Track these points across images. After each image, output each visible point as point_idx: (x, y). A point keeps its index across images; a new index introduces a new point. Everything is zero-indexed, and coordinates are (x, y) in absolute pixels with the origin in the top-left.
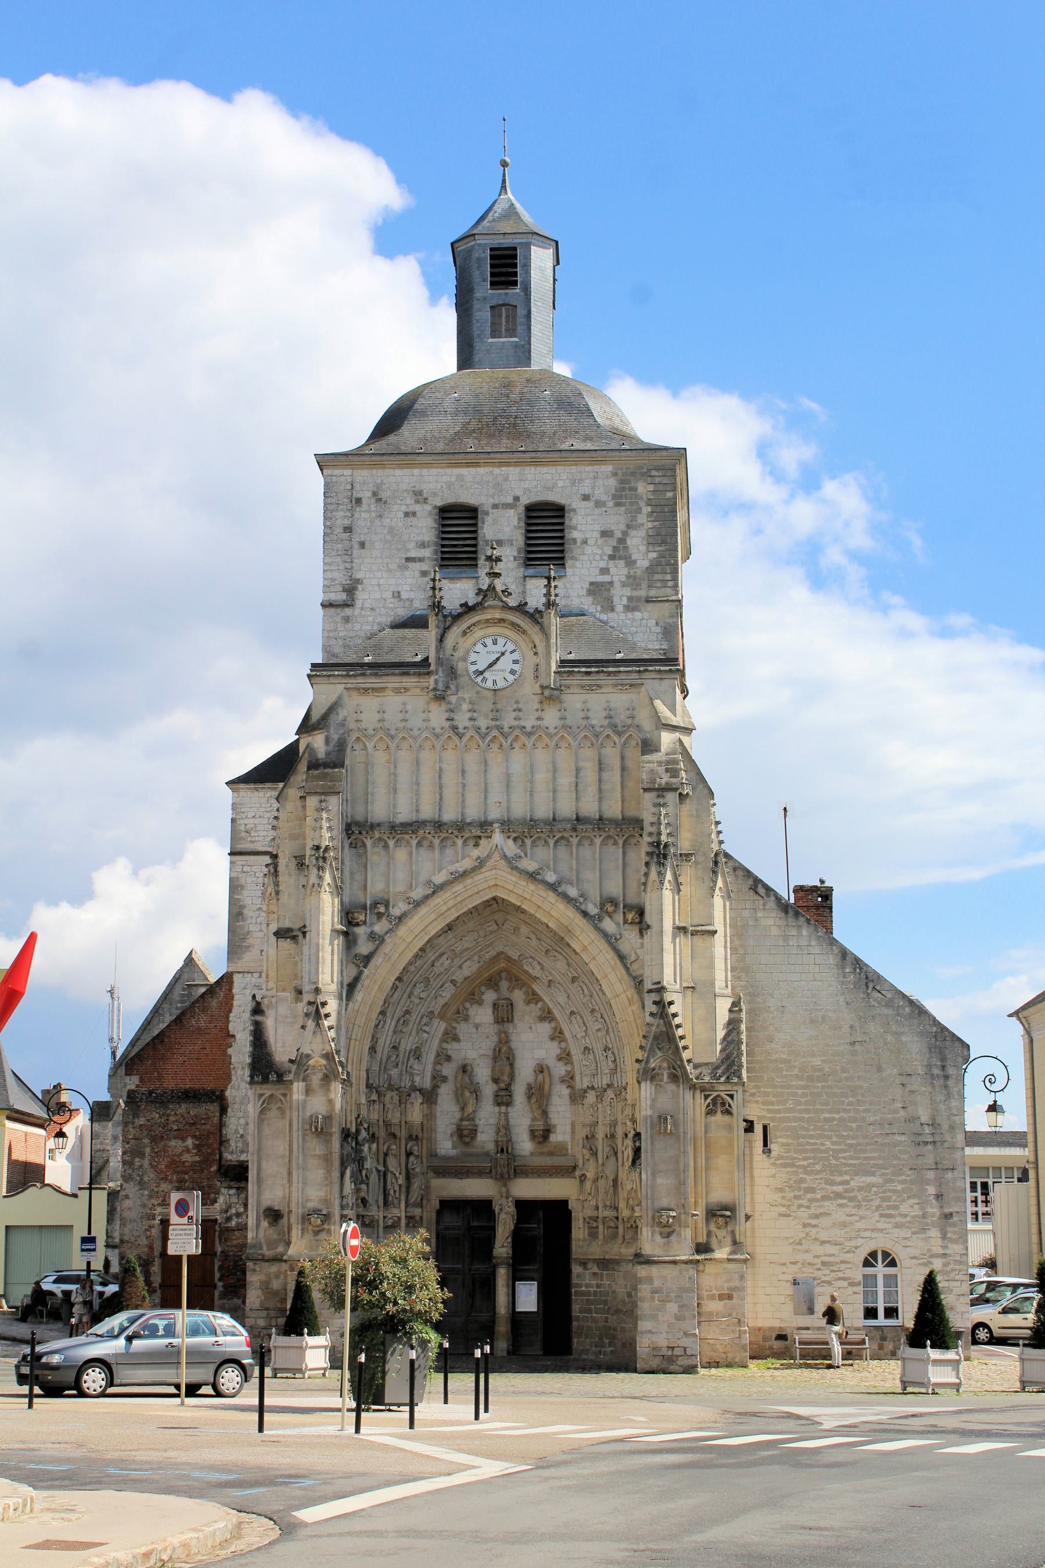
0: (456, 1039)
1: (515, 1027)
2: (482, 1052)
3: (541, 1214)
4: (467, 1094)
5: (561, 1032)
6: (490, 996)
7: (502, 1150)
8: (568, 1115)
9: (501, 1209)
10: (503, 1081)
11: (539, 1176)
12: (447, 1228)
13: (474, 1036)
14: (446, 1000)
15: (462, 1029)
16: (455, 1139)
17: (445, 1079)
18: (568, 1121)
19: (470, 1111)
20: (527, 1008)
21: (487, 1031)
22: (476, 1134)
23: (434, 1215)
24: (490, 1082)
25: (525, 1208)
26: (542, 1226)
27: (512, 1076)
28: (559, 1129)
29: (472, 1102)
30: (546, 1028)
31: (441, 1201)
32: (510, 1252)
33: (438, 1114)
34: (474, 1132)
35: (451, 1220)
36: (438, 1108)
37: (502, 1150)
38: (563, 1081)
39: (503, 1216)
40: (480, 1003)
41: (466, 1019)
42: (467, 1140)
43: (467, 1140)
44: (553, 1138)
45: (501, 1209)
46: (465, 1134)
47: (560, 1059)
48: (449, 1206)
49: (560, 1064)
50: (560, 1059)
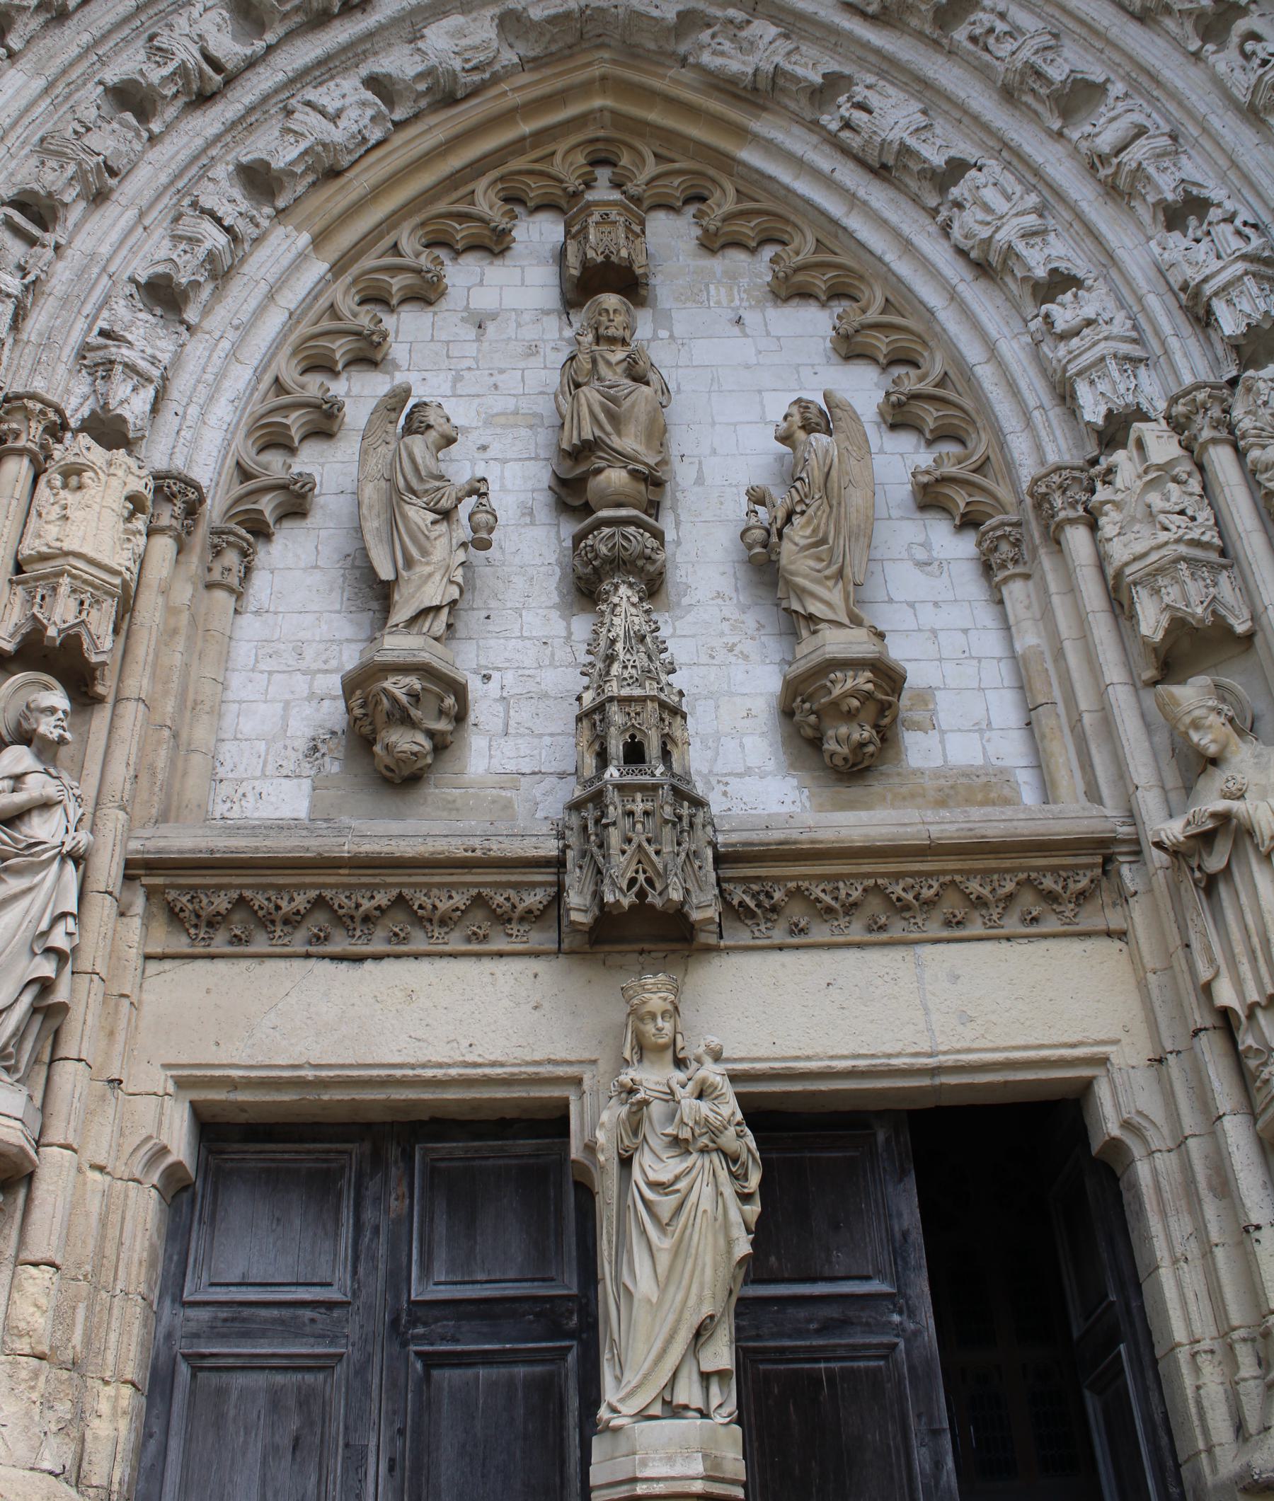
0: (369, 355)
1: (664, 319)
2: (500, 404)
3: (907, 1210)
4: (418, 515)
5: (899, 299)
6: (539, 234)
7: (635, 754)
8: (990, 643)
9: (635, 1122)
10: (623, 458)
11: (878, 937)
12: (237, 1318)
13: (471, 349)
14: (337, 134)
15: (407, 329)
16: (333, 767)
17: (296, 501)
18: (998, 674)
19: (434, 593)
20: (717, 264)
21: (530, 333)
22: (460, 717)
23: (143, 1209)
24: (544, 513)
25: (806, 1140)
26: (921, 1287)
27: (658, 433)
28: (947, 708)
29: (444, 546)
30: (814, 324)
31: (211, 1128)
32: (733, 1461)
33: (243, 652)
34: (449, 697)
35: (265, 1254)
36: (249, 626)
37: (635, 754)
38: (930, 496)
39: (655, 1165)
40: (494, 244)
41: (426, 293)
42: (406, 741)
43: (406, 741)
44: (919, 750)
45: (635, 1122)
46: (395, 727)
47: (899, 416)
48: (256, 1148)
49: (906, 442)
50: (899, 416)
